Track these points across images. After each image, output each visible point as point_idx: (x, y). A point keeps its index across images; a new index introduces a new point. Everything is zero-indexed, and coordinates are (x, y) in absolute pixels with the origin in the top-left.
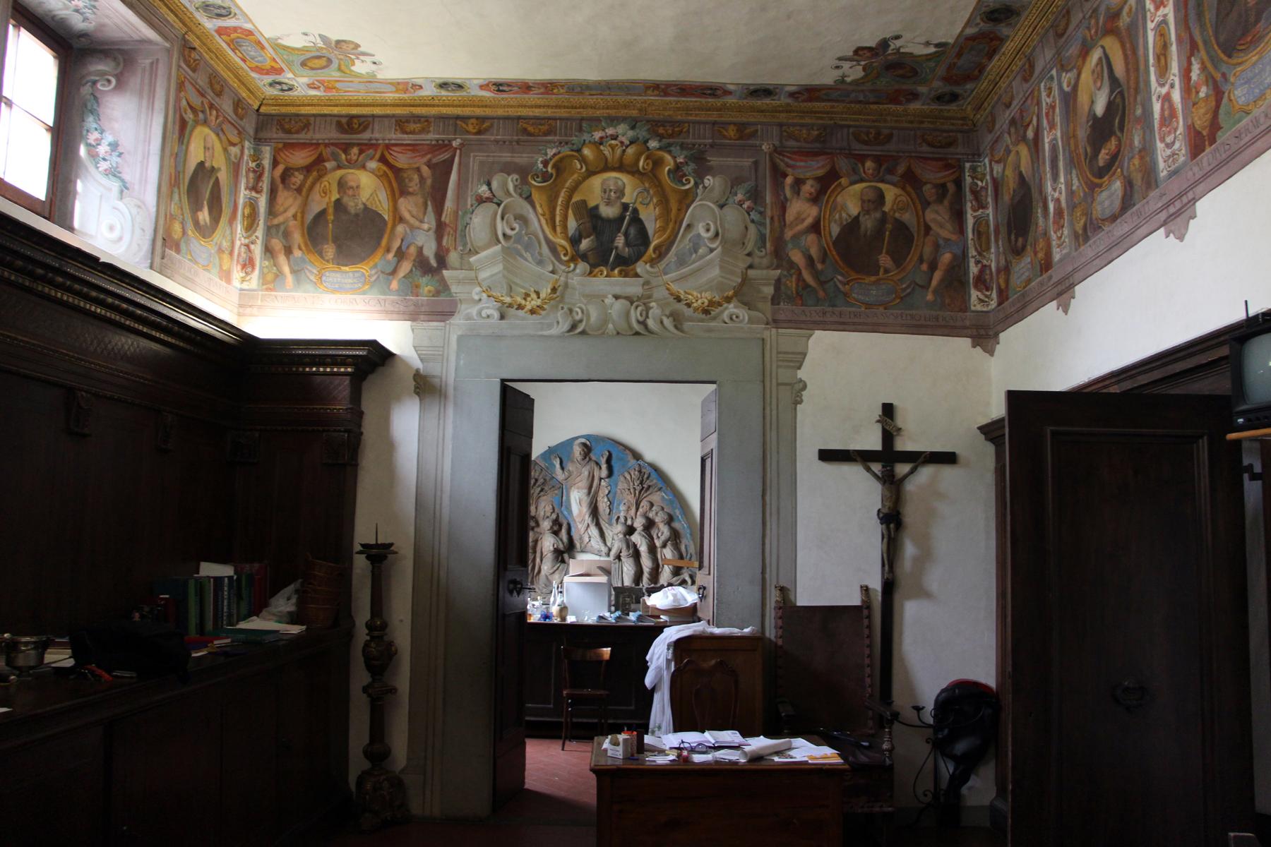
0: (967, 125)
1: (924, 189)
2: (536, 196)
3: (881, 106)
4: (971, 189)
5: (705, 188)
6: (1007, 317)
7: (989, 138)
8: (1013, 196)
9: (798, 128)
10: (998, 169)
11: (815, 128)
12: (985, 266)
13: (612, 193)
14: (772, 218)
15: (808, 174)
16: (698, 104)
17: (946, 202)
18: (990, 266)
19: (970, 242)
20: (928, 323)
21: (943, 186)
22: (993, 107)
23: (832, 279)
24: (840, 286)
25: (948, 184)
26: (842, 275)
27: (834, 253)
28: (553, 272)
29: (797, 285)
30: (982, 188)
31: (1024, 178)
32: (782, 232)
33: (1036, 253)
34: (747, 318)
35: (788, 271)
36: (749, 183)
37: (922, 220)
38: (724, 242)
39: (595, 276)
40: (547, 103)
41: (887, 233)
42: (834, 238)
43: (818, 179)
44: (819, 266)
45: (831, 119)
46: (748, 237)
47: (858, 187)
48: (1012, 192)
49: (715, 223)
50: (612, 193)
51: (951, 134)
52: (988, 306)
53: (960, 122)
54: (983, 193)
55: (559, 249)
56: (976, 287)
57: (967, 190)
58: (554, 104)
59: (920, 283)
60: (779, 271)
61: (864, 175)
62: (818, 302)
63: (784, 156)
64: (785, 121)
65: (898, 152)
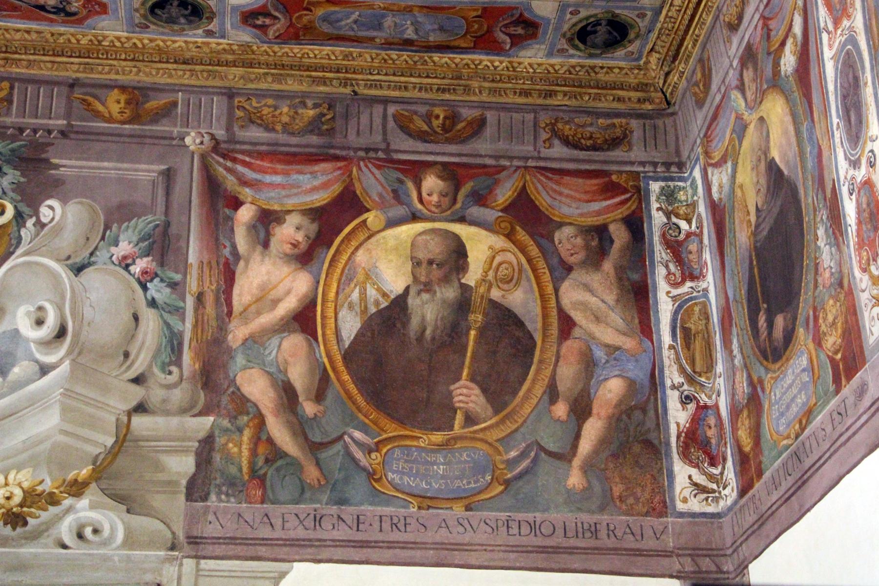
0: (650, 101)
1: (557, 236)
3: (458, 57)
4: (663, 235)
5: (40, 225)
6: (762, 521)
7: (699, 120)
8: (757, 226)
9: (270, 101)
10: (719, 178)
11: (310, 103)
12: (706, 407)
14: (200, 298)
15: (290, 202)
16: (34, 36)
17: (608, 266)
18: (716, 406)
19: (666, 353)
20: (573, 542)
21: (601, 231)
22: (704, 47)
23: (340, 438)
24: (359, 455)
25: (612, 228)
26: (364, 429)
27: (346, 377)
29: (254, 453)
30: (689, 235)
31: (779, 171)
32: (222, 328)
33: (818, 342)
34: (120, 535)
35: (233, 418)
36: (150, 218)
37: (553, 303)
38: (77, 352)
41: (473, 333)
42: (347, 344)
43: (316, 214)
44: (309, 408)
45: (345, 83)
46: (140, 336)
47: (408, 231)
48: (753, 218)
49: (60, 308)
51: (616, 121)
52: (716, 500)
53: (634, 95)
54: (693, 247)
56: (685, 455)
57: (656, 239)
59: (552, 447)
60: (212, 419)
61: (419, 206)
62: (303, 492)
63: (234, 160)
64: (240, 84)
65: (497, 157)
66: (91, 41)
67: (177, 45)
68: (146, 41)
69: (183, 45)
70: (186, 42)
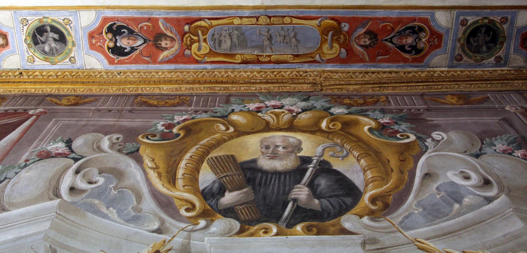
2: (145, 153)
13: (280, 149)
16: (394, 75)
28: (159, 231)
39: (252, 235)
40: (181, 77)
50: (280, 149)
55: (177, 203)
58: (191, 78)
66: (427, 74)
67: (477, 73)
70: (482, 71)
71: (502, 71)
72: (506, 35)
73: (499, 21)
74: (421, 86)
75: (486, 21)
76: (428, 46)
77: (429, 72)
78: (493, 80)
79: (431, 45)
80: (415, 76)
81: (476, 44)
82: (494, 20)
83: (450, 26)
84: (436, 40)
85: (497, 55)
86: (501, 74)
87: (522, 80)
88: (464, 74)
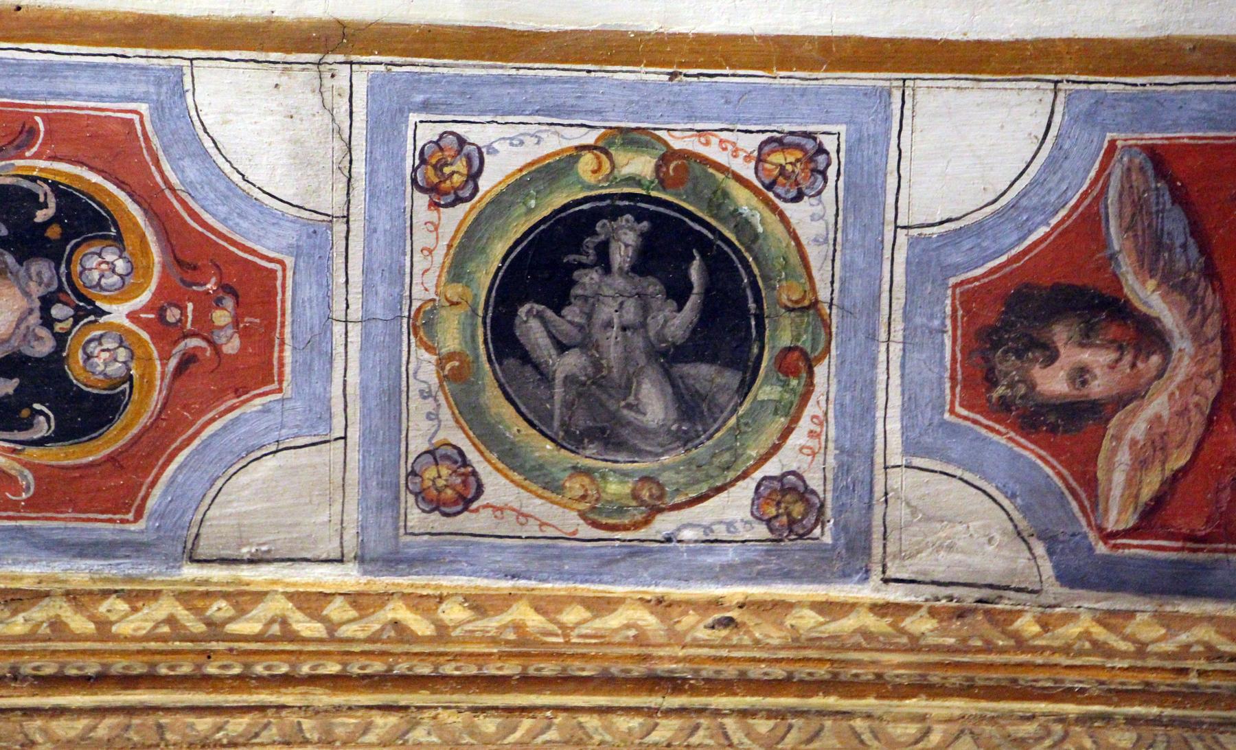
66: (171, 620)
67: (613, 621)
68: (453, 613)
69: (649, 620)
70: (660, 605)
71: (827, 608)
72: (824, 294)
73: (748, 172)
74: (80, 712)
75: (640, 165)
76: (162, 370)
77: (192, 597)
78: (716, 685)
79: (188, 360)
80: (57, 626)
81: (572, 363)
82: (705, 161)
83: (331, 201)
84: (222, 317)
85: (772, 468)
86: (813, 642)
87: (967, 691)
88: (492, 624)
